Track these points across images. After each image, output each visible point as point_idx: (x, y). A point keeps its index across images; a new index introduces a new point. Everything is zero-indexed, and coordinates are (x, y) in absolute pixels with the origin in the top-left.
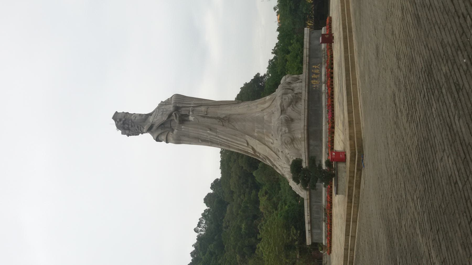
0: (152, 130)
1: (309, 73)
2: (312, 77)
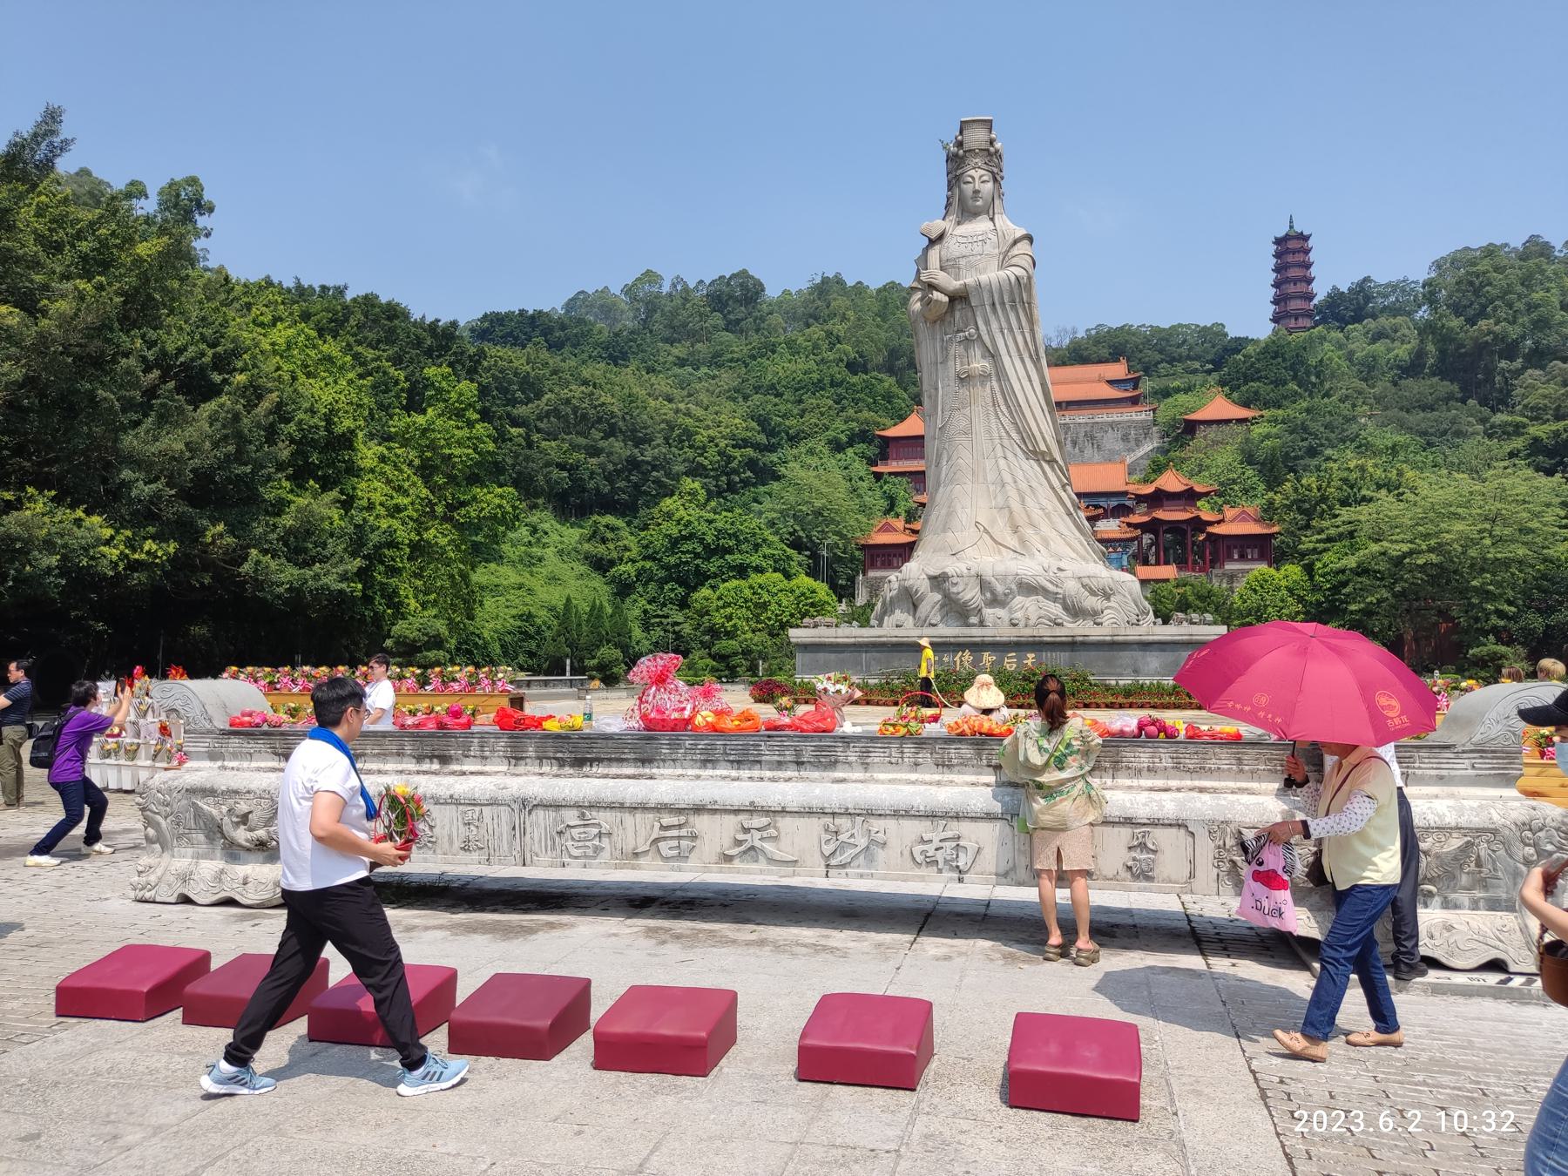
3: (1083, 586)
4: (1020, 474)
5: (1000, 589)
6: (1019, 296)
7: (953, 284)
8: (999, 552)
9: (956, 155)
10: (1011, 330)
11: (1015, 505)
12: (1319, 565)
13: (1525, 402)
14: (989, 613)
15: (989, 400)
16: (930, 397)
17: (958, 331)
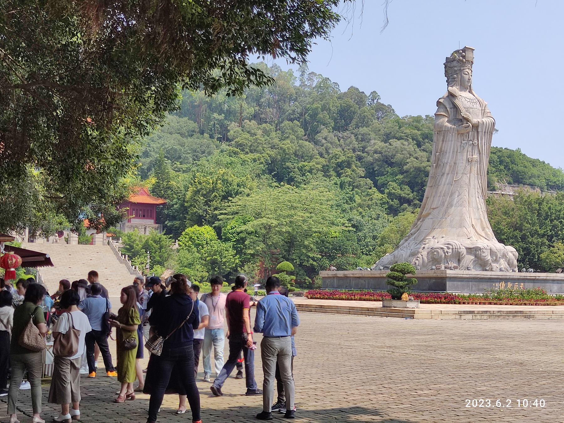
0: (450, 97)
1: (518, 279)
2: (509, 283)
3: (514, 255)
4: (482, 204)
5: (499, 255)
6: (491, 129)
7: (475, 120)
8: (480, 238)
9: (462, 61)
10: (487, 144)
11: (483, 219)
12: (229, 227)
13: (237, 140)
14: (494, 265)
15: (476, 172)
16: (450, 167)
17: (471, 141)
